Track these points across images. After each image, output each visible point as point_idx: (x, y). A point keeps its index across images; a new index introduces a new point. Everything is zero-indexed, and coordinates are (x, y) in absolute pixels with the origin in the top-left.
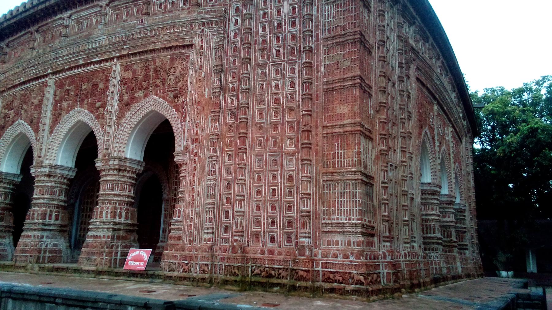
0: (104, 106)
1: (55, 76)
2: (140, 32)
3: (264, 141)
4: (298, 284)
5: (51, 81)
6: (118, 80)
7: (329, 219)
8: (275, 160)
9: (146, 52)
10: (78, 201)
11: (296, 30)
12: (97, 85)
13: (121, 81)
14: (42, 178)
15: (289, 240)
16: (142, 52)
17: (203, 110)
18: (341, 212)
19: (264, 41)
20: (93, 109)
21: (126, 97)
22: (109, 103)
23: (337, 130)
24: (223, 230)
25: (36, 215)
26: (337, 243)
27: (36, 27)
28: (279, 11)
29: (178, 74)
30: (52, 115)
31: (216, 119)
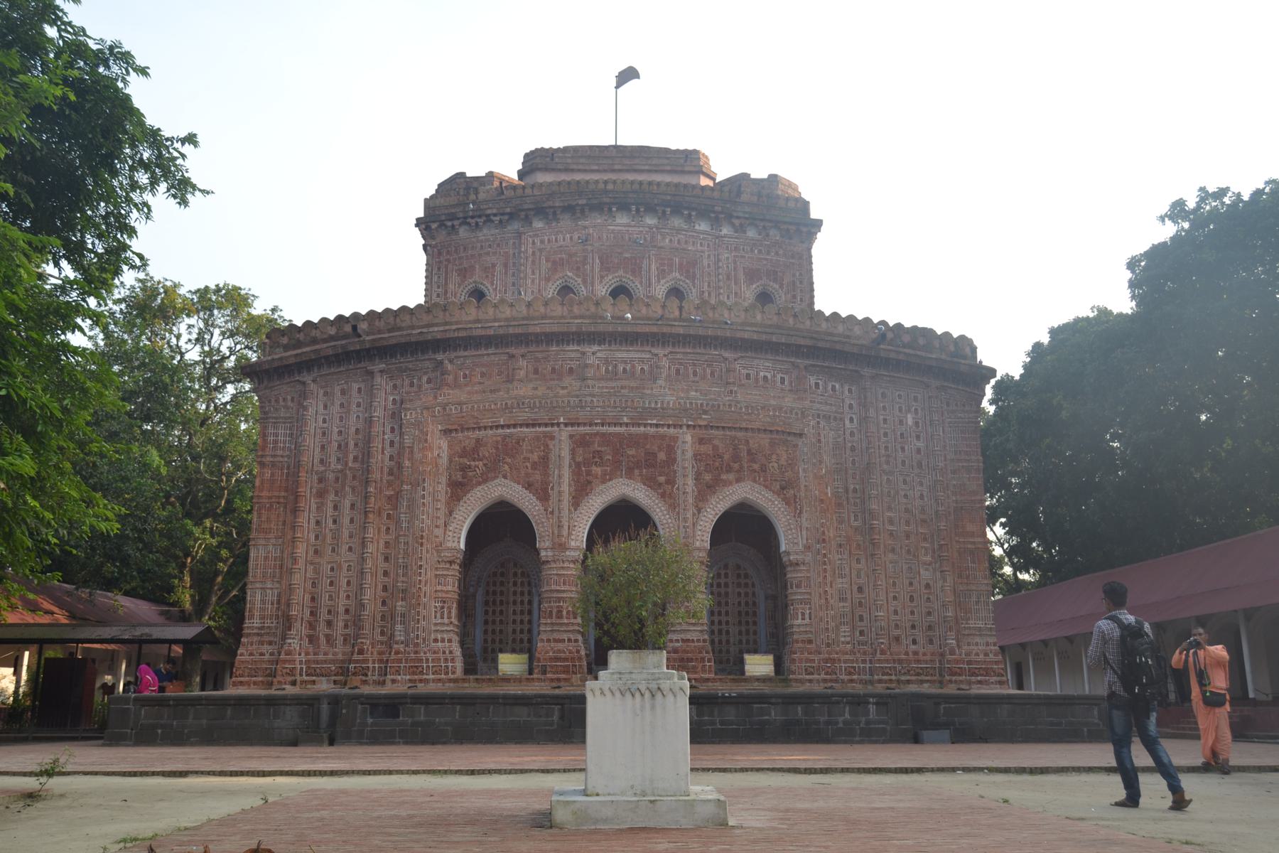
0: (671, 482)
2: (730, 406)
5: (564, 434)
6: (689, 454)
8: (910, 568)
10: (481, 591)
11: (920, 444)
12: (655, 455)
13: (695, 455)
14: (566, 565)
15: (931, 642)
19: (886, 448)
20: (651, 482)
21: (707, 477)
22: (680, 481)
26: (977, 644)
27: (523, 350)
28: (901, 421)
29: (783, 462)
31: (841, 522)
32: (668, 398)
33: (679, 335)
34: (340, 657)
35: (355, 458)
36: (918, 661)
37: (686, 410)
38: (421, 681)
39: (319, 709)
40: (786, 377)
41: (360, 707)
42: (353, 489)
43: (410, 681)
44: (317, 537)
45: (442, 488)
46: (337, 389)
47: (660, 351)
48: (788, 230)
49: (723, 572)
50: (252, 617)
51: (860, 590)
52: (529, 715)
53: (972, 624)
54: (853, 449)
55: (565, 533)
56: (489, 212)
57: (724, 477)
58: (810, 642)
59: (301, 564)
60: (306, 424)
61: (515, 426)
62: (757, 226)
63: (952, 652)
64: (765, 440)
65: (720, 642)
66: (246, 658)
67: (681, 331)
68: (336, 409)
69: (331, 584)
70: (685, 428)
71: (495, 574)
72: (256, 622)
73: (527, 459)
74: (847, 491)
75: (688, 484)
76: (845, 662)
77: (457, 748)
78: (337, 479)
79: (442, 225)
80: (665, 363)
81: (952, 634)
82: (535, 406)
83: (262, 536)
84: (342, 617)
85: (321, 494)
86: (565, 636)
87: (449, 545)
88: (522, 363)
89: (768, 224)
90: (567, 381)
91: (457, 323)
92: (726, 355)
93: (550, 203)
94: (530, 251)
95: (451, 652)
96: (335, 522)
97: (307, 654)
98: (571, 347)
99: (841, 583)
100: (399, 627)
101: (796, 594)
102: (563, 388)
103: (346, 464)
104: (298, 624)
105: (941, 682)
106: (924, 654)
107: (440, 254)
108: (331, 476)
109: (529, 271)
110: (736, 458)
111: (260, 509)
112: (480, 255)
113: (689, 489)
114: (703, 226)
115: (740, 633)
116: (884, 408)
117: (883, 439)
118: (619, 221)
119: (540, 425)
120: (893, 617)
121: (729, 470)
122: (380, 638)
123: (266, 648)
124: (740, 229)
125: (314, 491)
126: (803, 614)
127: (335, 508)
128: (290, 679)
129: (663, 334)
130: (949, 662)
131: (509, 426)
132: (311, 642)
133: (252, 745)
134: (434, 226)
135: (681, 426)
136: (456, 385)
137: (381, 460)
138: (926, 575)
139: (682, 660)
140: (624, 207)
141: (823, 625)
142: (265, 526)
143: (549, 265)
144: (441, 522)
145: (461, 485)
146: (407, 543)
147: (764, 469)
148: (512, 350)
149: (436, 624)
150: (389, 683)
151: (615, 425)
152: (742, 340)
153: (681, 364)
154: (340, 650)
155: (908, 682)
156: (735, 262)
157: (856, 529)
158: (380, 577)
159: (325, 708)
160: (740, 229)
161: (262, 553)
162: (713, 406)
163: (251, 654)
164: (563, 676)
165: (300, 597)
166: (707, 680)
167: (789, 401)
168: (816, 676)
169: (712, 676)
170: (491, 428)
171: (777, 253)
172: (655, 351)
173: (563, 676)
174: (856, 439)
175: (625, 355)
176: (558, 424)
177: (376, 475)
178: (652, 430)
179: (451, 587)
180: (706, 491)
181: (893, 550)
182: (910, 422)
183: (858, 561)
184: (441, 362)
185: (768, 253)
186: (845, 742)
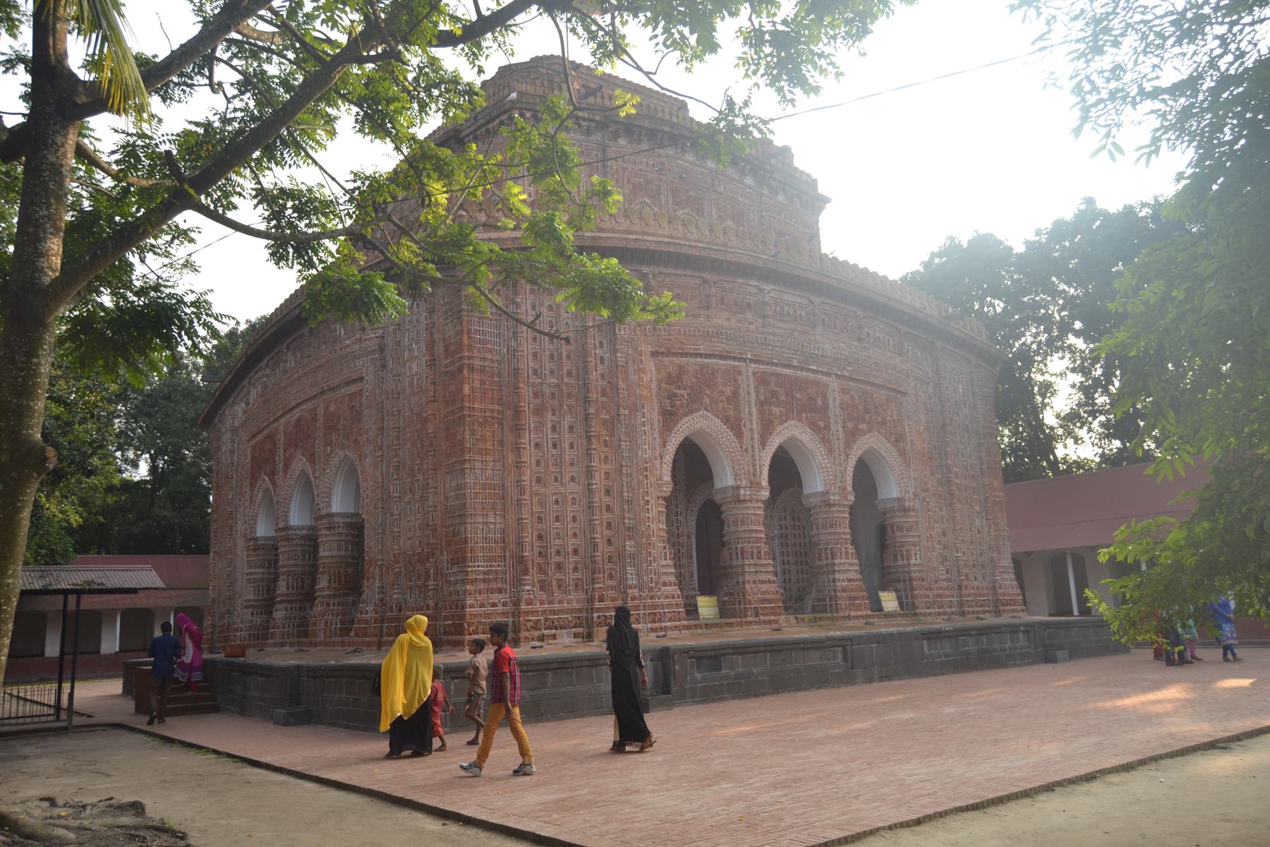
0: (827, 427)
20: (813, 426)
22: (833, 428)
34: (575, 605)
44: (538, 463)
66: (476, 610)
75: (837, 429)
77: (773, 697)
83: (478, 457)
85: (539, 411)
90: (749, 315)
91: (653, 235)
92: (859, 312)
97: (542, 603)
98: (751, 283)
100: (630, 569)
119: (730, 358)
122: (610, 583)
123: (496, 597)
127: (554, 429)
132: (542, 588)
133: (582, 716)
139: (851, 598)
142: (481, 445)
145: (671, 414)
154: (574, 599)
163: (482, 605)
164: (772, 618)
169: (869, 613)
172: (813, 298)
173: (772, 618)
176: (744, 360)
177: (593, 396)
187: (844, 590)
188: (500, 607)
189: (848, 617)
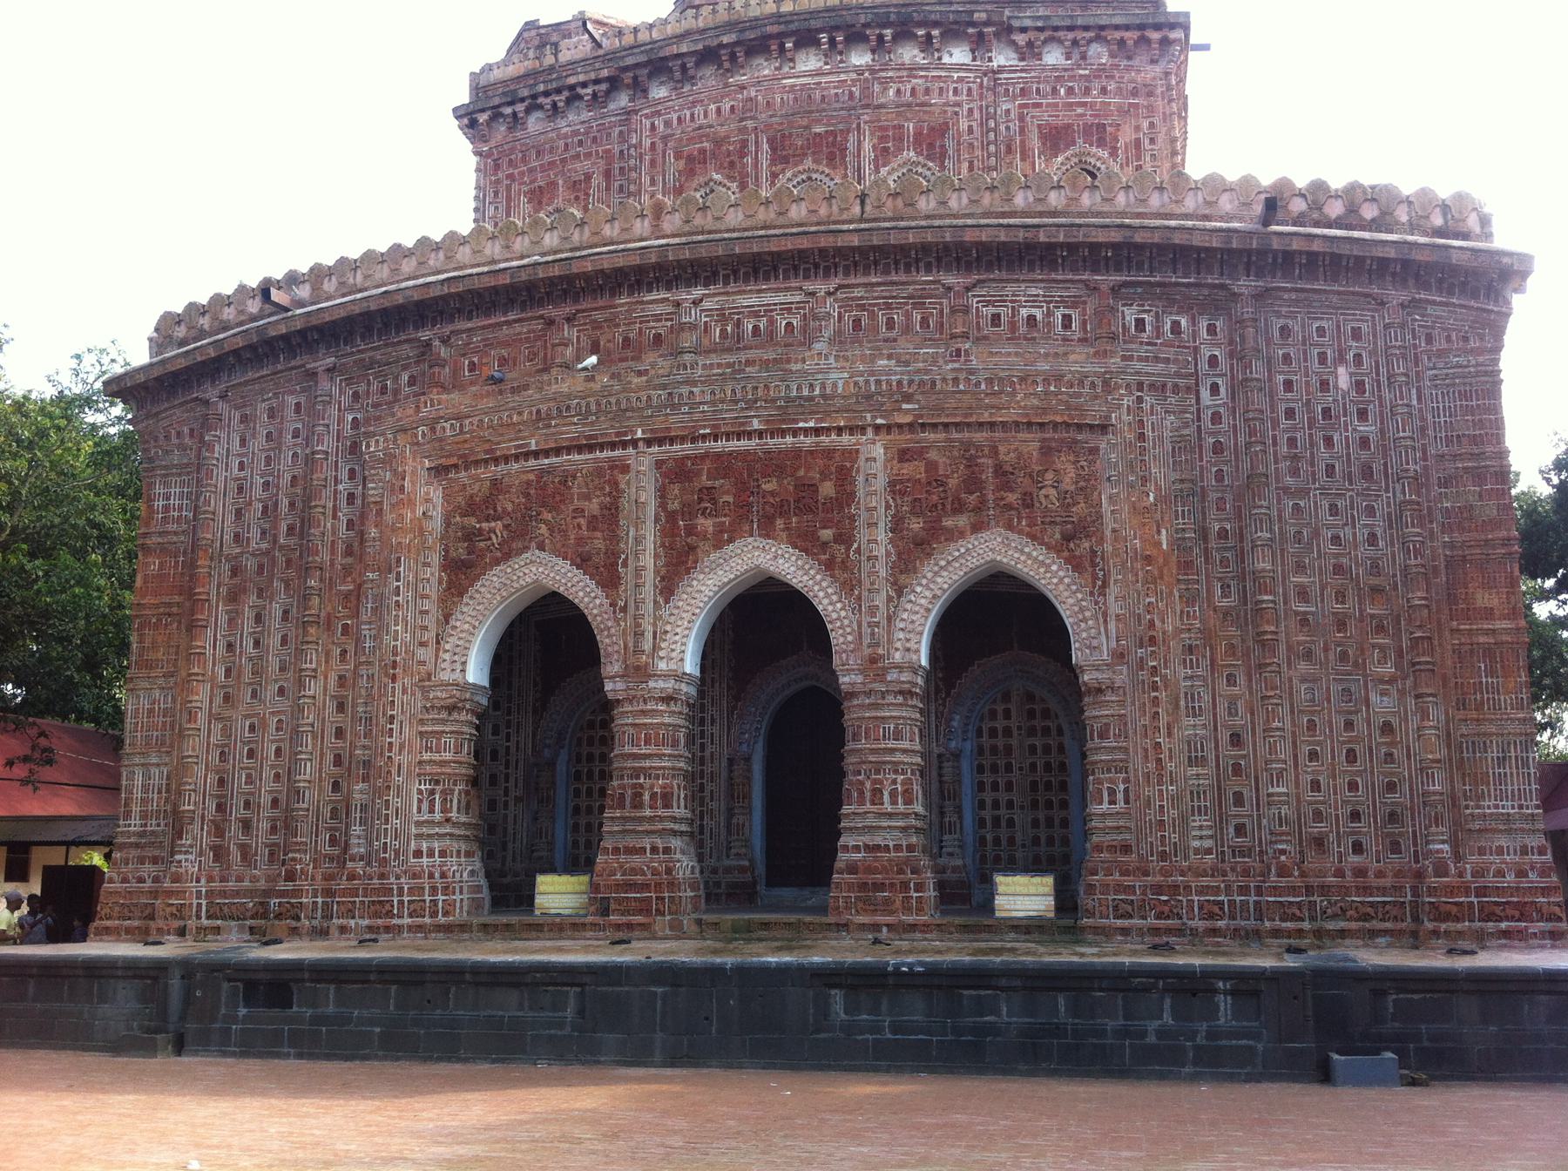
0: (845, 538)
1: (655, 449)
2: (956, 380)
3: (1318, 651)
4: (1443, 926)
5: (643, 462)
6: (880, 483)
7: (1478, 807)
8: (1347, 691)
9: (969, 425)
10: (563, 756)
12: (813, 488)
13: (892, 484)
15: (1395, 848)
16: (956, 425)
17: (1161, 578)
18: (1502, 796)
19: (1292, 442)
20: (806, 543)
21: (916, 525)
22: (862, 536)
23: (1482, 639)
24: (1232, 830)
25: (646, 797)
27: (568, 309)
28: (1324, 385)
29: (1068, 484)
30: (663, 545)
31: (1189, 599)
32: (833, 376)
33: (853, 249)
34: (262, 885)
35: (291, 529)
36: (1366, 890)
37: (869, 397)
38: (388, 929)
39: (166, 985)
40: (1075, 315)
41: (225, 985)
42: (287, 586)
43: (370, 928)
44: (228, 672)
45: (433, 573)
46: (262, 407)
47: (820, 287)
48: (1122, 42)
49: (1000, 708)
50: (128, 815)
51: (1236, 740)
52: (521, 1007)
53: (1488, 806)
54: (1218, 448)
55: (647, 645)
56: (572, 80)
57: (948, 522)
58: (1126, 849)
59: (202, 718)
60: (209, 475)
61: (557, 451)
62: (1060, 41)
63: (1441, 870)
64: (1030, 444)
65: (997, 841)
67: (855, 241)
68: (258, 443)
69: (251, 754)
70: (870, 433)
71: (591, 725)
72: (135, 824)
73: (579, 511)
74: (1204, 534)
75: (876, 541)
76: (1202, 891)
78: (261, 567)
79: (496, 115)
80: (831, 307)
81: (1443, 830)
82: (588, 412)
84: (266, 813)
85: (234, 597)
86: (646, 843)
87: (445, 676)
88: (570, 333)
89: (1080, 35)
90: (650, 357)
92: (950, 280)
93: (675, 50)
94: (647, 143)
95: (443, 875)
96: (257, 644)
97: (210, 879)
98: (654, 296)
99: (1190, 727)
100: (357, 830)
101: (1101, 753)
102: (640, 373)
103: (275, 542)
104: (196, 826)
105: (1414, 934)
106: (1380, 874)
107: (497, 167)
108: (250, 564)
109: (646, 180)
110: (973, 483)
111: (142, 627)
112: (564, 161)
113: (880, 551)
114: (958, 55)
115: (1035, 823)
116: (1286, 357)
117: (1285, 423)
118: (802, 67)
119: (602, 447)
120: (1309, 796)
121: (959, 508)
123: (148, 869)
124: (1030, 52)
125: (224, 590)
126: (1112, 792)
127: (258, 619)
128: (177, 924)
129: (823, 252)
130: (1432, 891)
131: (547, 453)
132: (217, 858)
134: (483, 118)
135: (863, 430)
136: (457, 385)
137: (332, 527)
138: (1382, 704)
139: (863, 886)
140: (807, 39)
141: (1152, 815)
142: (151, 656)
143: (682, 163)
144: (430, 636)
146: (371, 677)
147: (1028, 501)
148: (549, 311)
149: (419, 824)
150: (334, 932)
151: (739, 436)
152: (979, 245)
153: (862, 308)
155: (1343, 934)
156: (1022, 118)
157: (1226, 613)
158: (330, 739)
159: (175, 983)
160: (1030, 52)
161: (145, 704)
162: (922, 383)
163: (125, 880)
164: (639, 919)
165: (201, 777)
166: (913, 927)
167: (1079, 361)
168: (1136, 922)
170: (517, 457)
171: (1104, 91)
172: (809, 286)
173: (639, 919)
174: (1224, 426)
175: (753, 300)
177: (324, 556)
178: (807, 441)
179: (452, 751)
180: (912, 552)
181: (1308, 655)
182: (1343, 378)
183: (1231, 680)
184: (428, 344)
185: (1087, 91)
186: (1162, 1077)
187: (852, 868)
188: (149, 884)
189: (845, 926)
